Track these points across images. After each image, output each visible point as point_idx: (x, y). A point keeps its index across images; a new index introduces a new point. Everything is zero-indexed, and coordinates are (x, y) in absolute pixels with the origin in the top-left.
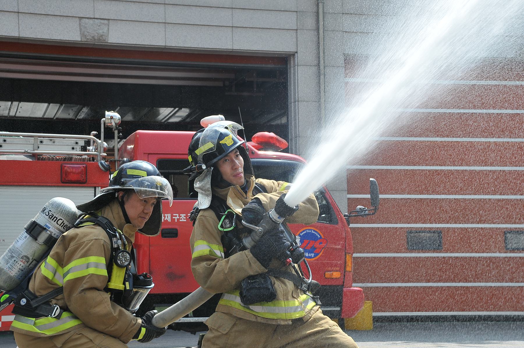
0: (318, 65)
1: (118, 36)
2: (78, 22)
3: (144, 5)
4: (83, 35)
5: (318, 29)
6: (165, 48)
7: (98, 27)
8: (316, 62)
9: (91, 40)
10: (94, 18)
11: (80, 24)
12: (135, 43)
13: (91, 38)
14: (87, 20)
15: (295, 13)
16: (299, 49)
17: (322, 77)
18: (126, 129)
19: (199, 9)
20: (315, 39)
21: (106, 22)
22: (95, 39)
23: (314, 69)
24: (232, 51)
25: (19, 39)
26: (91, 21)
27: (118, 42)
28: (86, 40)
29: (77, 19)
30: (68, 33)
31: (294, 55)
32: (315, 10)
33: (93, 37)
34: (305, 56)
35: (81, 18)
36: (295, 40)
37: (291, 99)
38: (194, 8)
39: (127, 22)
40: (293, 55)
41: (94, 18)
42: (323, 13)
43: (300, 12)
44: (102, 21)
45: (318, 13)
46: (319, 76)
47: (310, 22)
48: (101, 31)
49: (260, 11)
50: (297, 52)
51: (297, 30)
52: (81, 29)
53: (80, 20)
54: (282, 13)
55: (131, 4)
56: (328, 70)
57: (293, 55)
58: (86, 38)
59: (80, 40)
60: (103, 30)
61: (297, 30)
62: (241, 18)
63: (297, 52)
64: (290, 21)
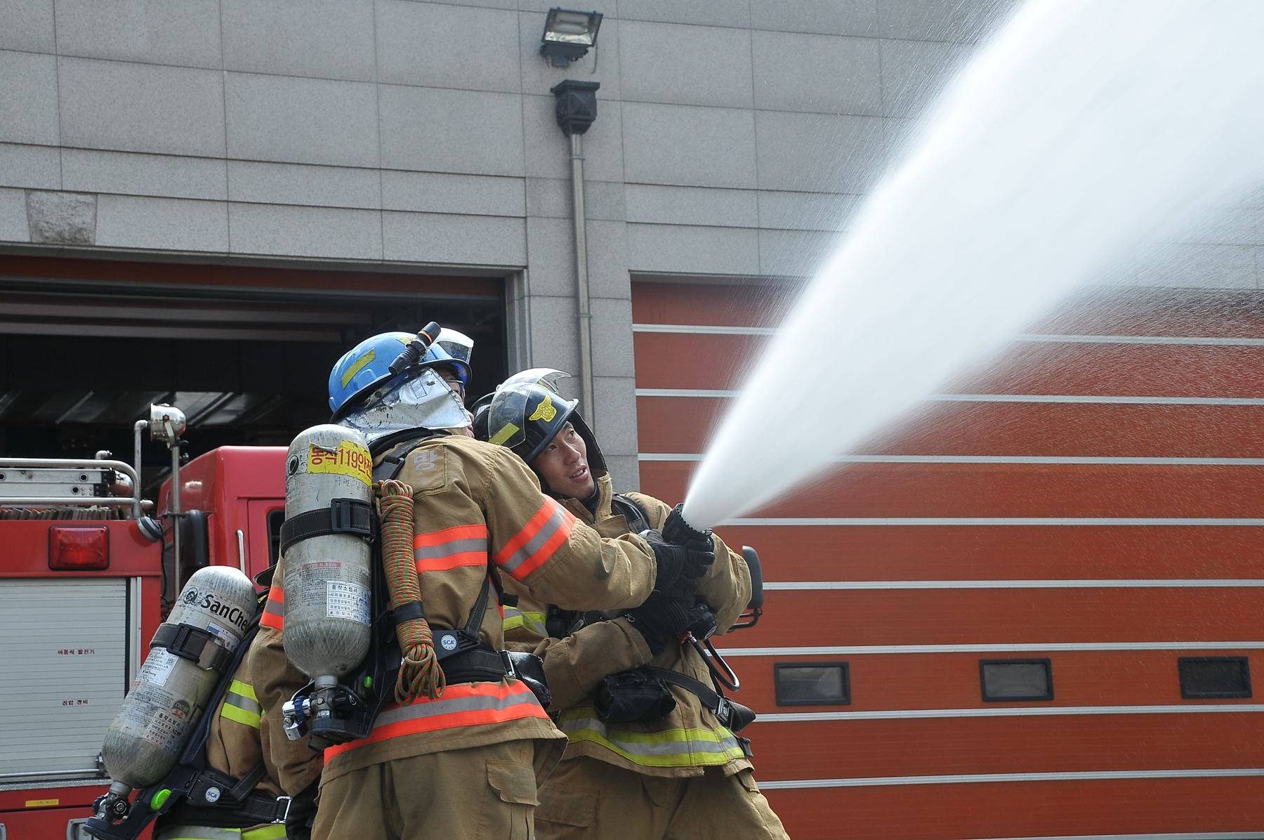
0: (576, 297)
2: (23, 199)
3: (179, 161)
4: (35, 228)
5: (572, 217)
6: (228, 257)
7: (70, 212)
8: (568, 290)
9: (55, 239)
10: (62, 191)
11: (28, 204)
12: (158, 247)
13: (54, 235)
14: (44, 195)
15: (521, 181)
16: (531, 259)
17: (584, 322)
19: (305, 170)
20: (566, 238)
21: (89, 199)
22: (63, 239)
23: (565, 306)
24: (383, 264)
26: (55, 198)
27: (117, 245)
28: (41, 240)
29: (22, 194)
33: (60, 234)
34: (544, 277)
36: (521, 240)
38: (293, 169)
39: (140, 200)
40: (517, 273)
41: (62, 191)
42: (584, 181)
43: (531, 178)
44: (80, 197)
45: (570, 182)
47: (554, 200)
48: (78, 221)
49: (443, 177)
50: (526, 267)
51: (525, 218)
52: (29, 217)
53: (28, 196)
54: (492, 180)
55: (146, 158)
56: (594, 303)
57: (517, 273)
58: (42, 235)
59: (27, 240)
60: (83, 218)
61: (525, 218)
62: (400, 192)
63: (526, 267)
64: (509, 198)
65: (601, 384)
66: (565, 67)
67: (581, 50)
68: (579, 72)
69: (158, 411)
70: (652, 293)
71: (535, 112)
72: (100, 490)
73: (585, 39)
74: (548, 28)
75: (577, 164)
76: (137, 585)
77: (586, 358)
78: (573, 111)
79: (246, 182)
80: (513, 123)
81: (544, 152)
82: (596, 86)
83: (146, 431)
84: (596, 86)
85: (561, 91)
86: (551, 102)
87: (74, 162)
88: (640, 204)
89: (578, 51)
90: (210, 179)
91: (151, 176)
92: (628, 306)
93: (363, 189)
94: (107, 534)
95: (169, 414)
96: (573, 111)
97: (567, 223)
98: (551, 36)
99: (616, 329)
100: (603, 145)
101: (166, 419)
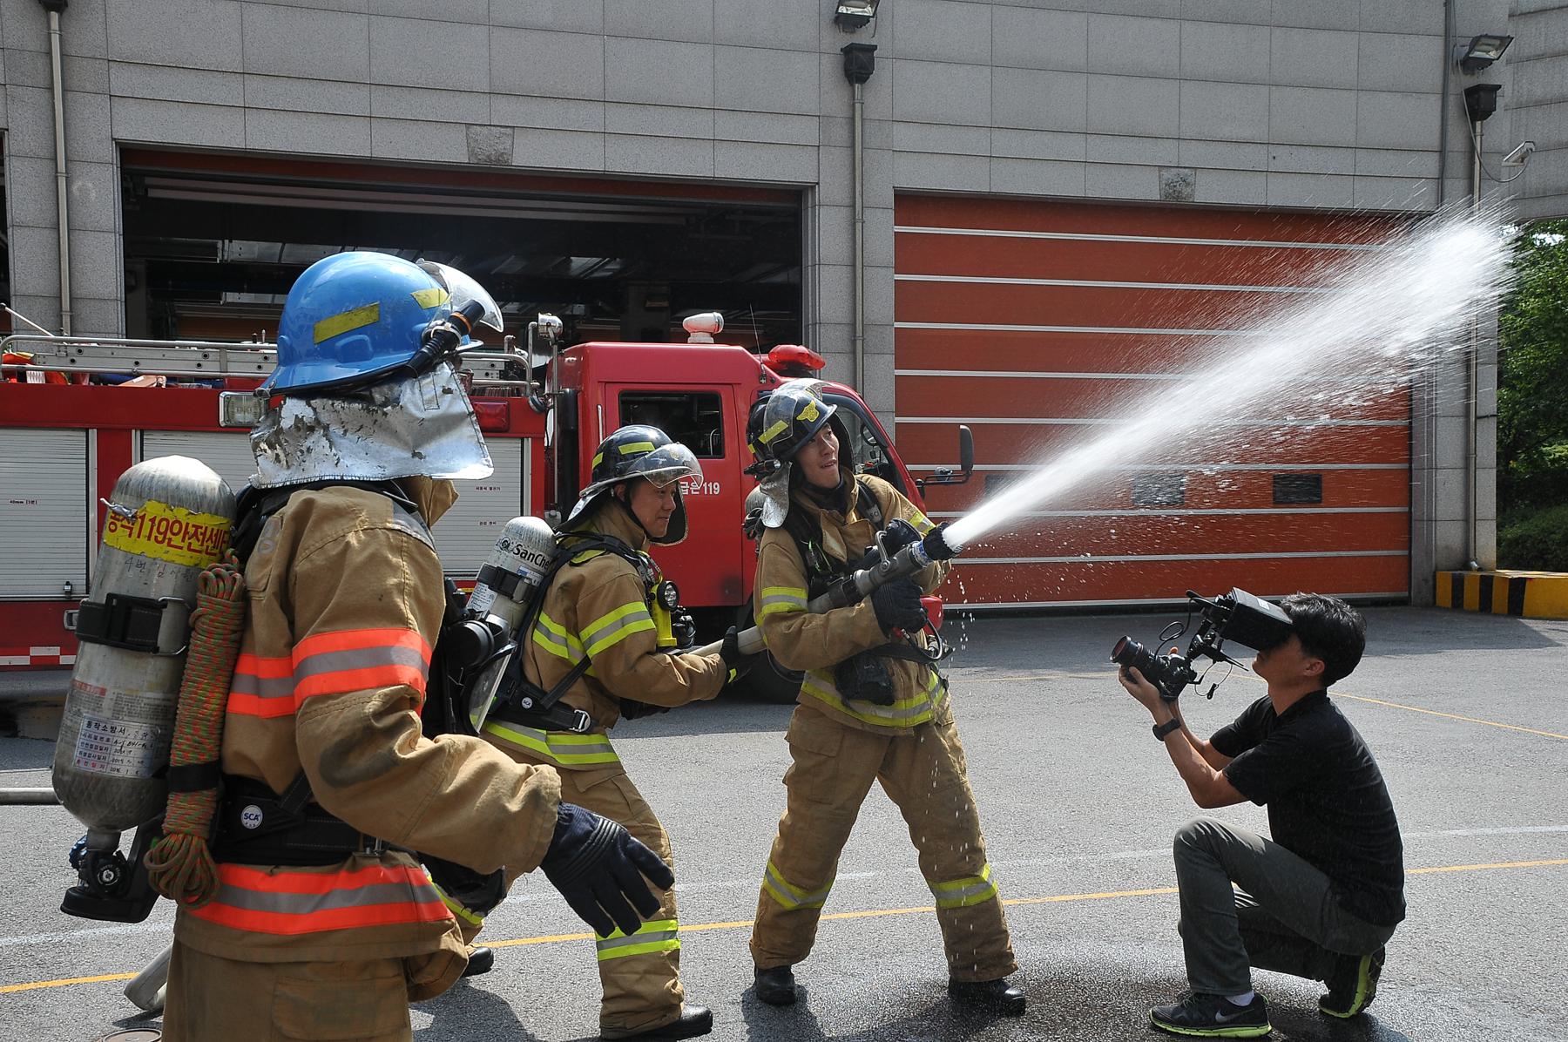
0: (853, 206)
1: (529, 154)
4: (472, 153)
8: (848, 201)
17: (859, 226)
18: (569, 337)
20: (848, 163)
21: (509, 131)
23: (844, 213)
25: (371, 159)
30: (448, 149)
31: (813, 188)
32: (849, 114)
35: (468, 125)
37: (808, 260)
40: (812, 187)
42: (863, 120)
45: (853, 118)
46: (854, 225)
47: (840, 133)
57: (812, 187)
62: (729, 126)
64: (807, 131)
65: (869, 272)
66: (853, 32)
67: (864, 20)
68: (862, 37)
69: (544, 318)
70: (910, 203)
71: (831, 66)
72: (503, 375)
73: (868, 11)
74: (841, 4)
75: (858, 106)
76: (528, 443)
77: (859, 253)
78: (857, 66)
79: (620, 119)
80: (812, 78)
81: (834, 96)
82: (875, 48)
83: (535, 329)
84: (875, 48)
85: (849, 51)
86: (841, 59)
87: (501, 104)
88: (904, 136)
89: (862, 21)
90: (591, 116)
91: (550, 114)
92: (891, 214)
93: (701, 124)
94: (507, 407)
95: (550, 320)
96: (857, 66)
97: (849, 151)
98: (843, 10)
99: (883, 230)
100: (879, 93)
101: (549, 325)
